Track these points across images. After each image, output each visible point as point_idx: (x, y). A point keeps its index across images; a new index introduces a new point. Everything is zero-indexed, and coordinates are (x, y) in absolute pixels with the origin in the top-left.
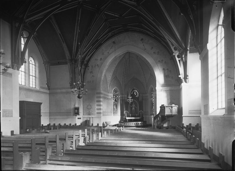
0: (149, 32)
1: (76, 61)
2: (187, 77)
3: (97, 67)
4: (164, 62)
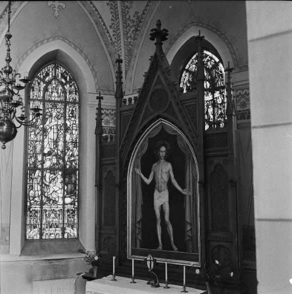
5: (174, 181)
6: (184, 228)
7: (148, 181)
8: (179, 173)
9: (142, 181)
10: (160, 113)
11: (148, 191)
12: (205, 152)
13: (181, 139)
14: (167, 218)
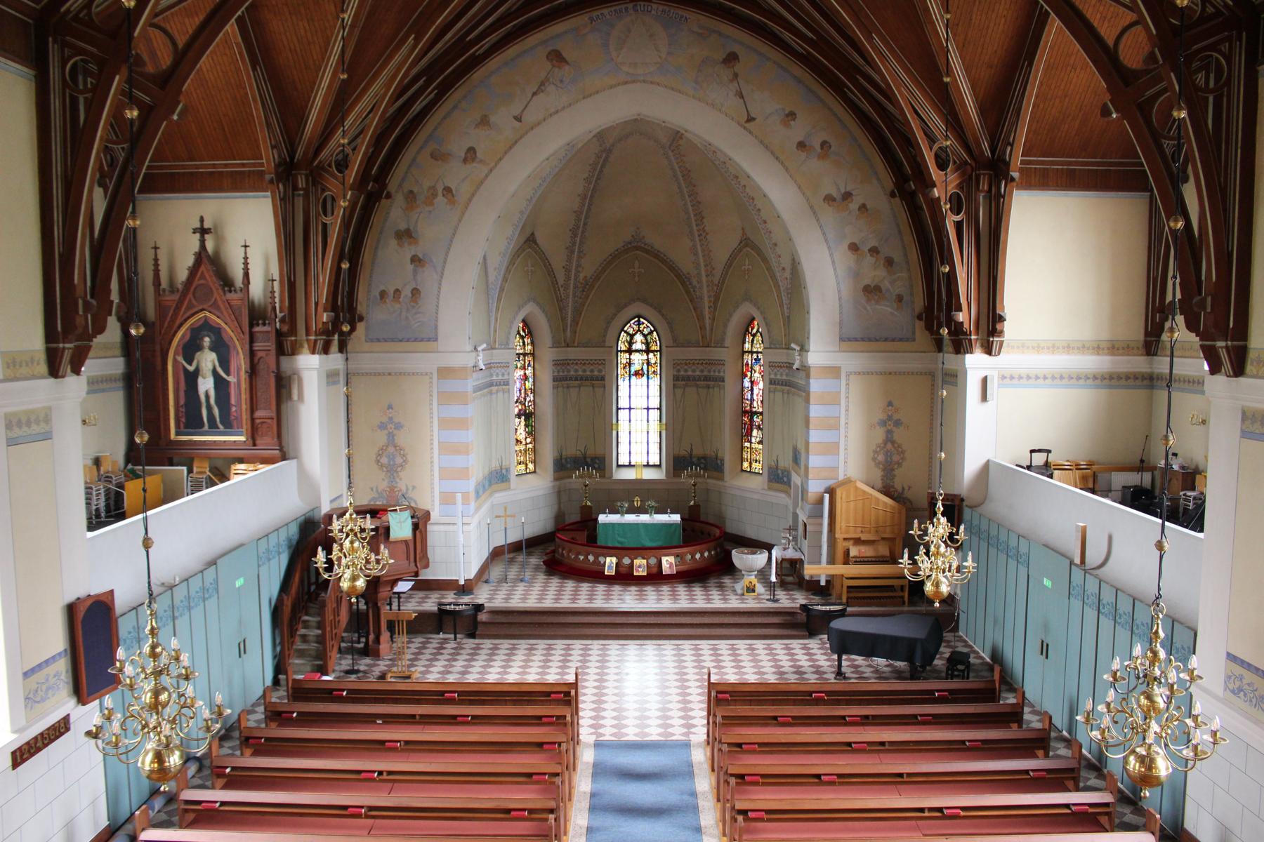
0: (787, 36)
1: (316, 176)
2: (998, 327)
3: (440, 200)
4: (854, 206)
6: (229, 409)
7: (191, 368)
8: (224, 362)
9: (185, 369)
10: (205, 306)
11: (192, 379)
12: (251, 347)
14: (212, 401)
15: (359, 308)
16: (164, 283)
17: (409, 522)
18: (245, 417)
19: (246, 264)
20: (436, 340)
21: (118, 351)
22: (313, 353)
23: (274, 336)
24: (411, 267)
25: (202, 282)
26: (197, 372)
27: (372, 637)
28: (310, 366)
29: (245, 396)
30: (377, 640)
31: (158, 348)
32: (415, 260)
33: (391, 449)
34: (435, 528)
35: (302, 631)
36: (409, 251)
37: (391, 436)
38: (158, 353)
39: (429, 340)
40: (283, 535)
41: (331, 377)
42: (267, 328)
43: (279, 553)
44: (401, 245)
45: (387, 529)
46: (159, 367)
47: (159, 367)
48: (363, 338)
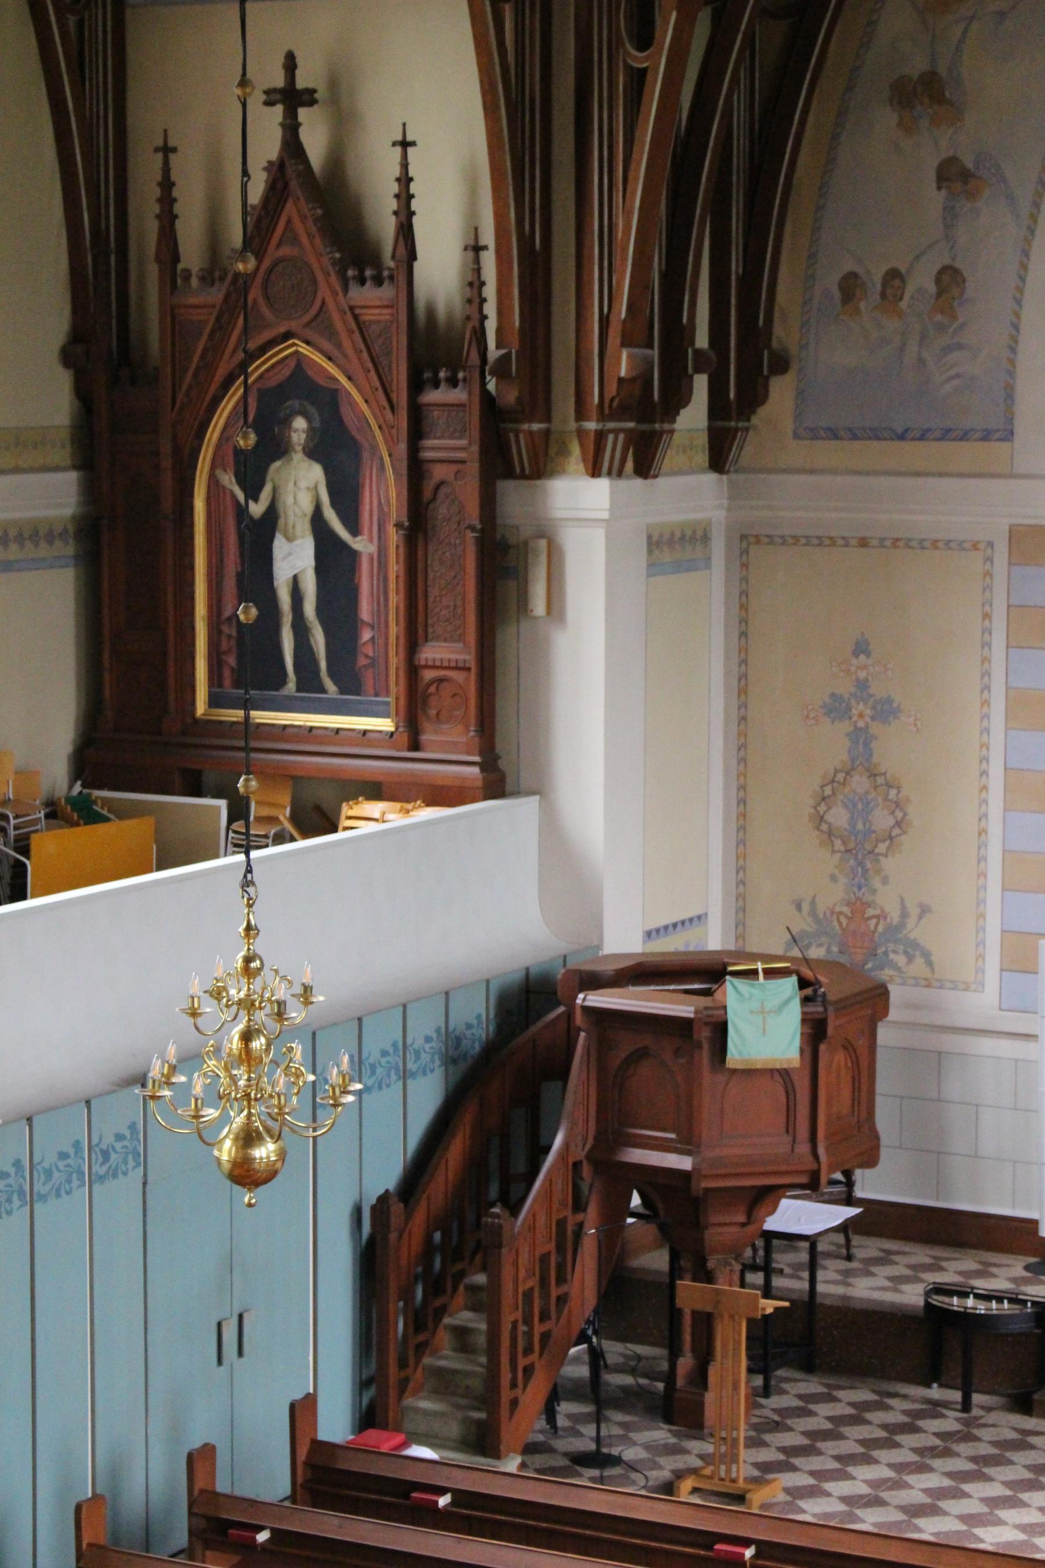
5: (331, 515)
6: (354, 635)
8: (345, 492)
9: (241, 512)
10: (294, 325)
11: (259, 536)
12: (414, 449)
13: (353, 404)
14: (310, 608)
15: (778, 330)
16: (192, 254)
17: (794, 1012)
18: (396, 661)
19: (405, 197)
20: (1008, 435)
21: (63, 455)
22: (595, 472)
23: (497, 411)
24: (935, 199)
25: (286, 251)
26: (271, 518)
27: (686, 1363)
28: (584, 509)
29: (396, 599)
30: (700, 1377)
31: (166, 447)
32: (955, 176)
33: (859, 783)
34: (987, 1046)
35: (465, 1317)
36: (930, 148)
37: (861, 740)
38: (167, 463)
39: (986, 436)
40: (425, 1026)
41: (671, 549)
42: (457, 395)
43: (405, 1075)
44: (907, 127)
45: (720, 1030)
46: (167, 504)
47: (167, 504)
48: (788, 425)
